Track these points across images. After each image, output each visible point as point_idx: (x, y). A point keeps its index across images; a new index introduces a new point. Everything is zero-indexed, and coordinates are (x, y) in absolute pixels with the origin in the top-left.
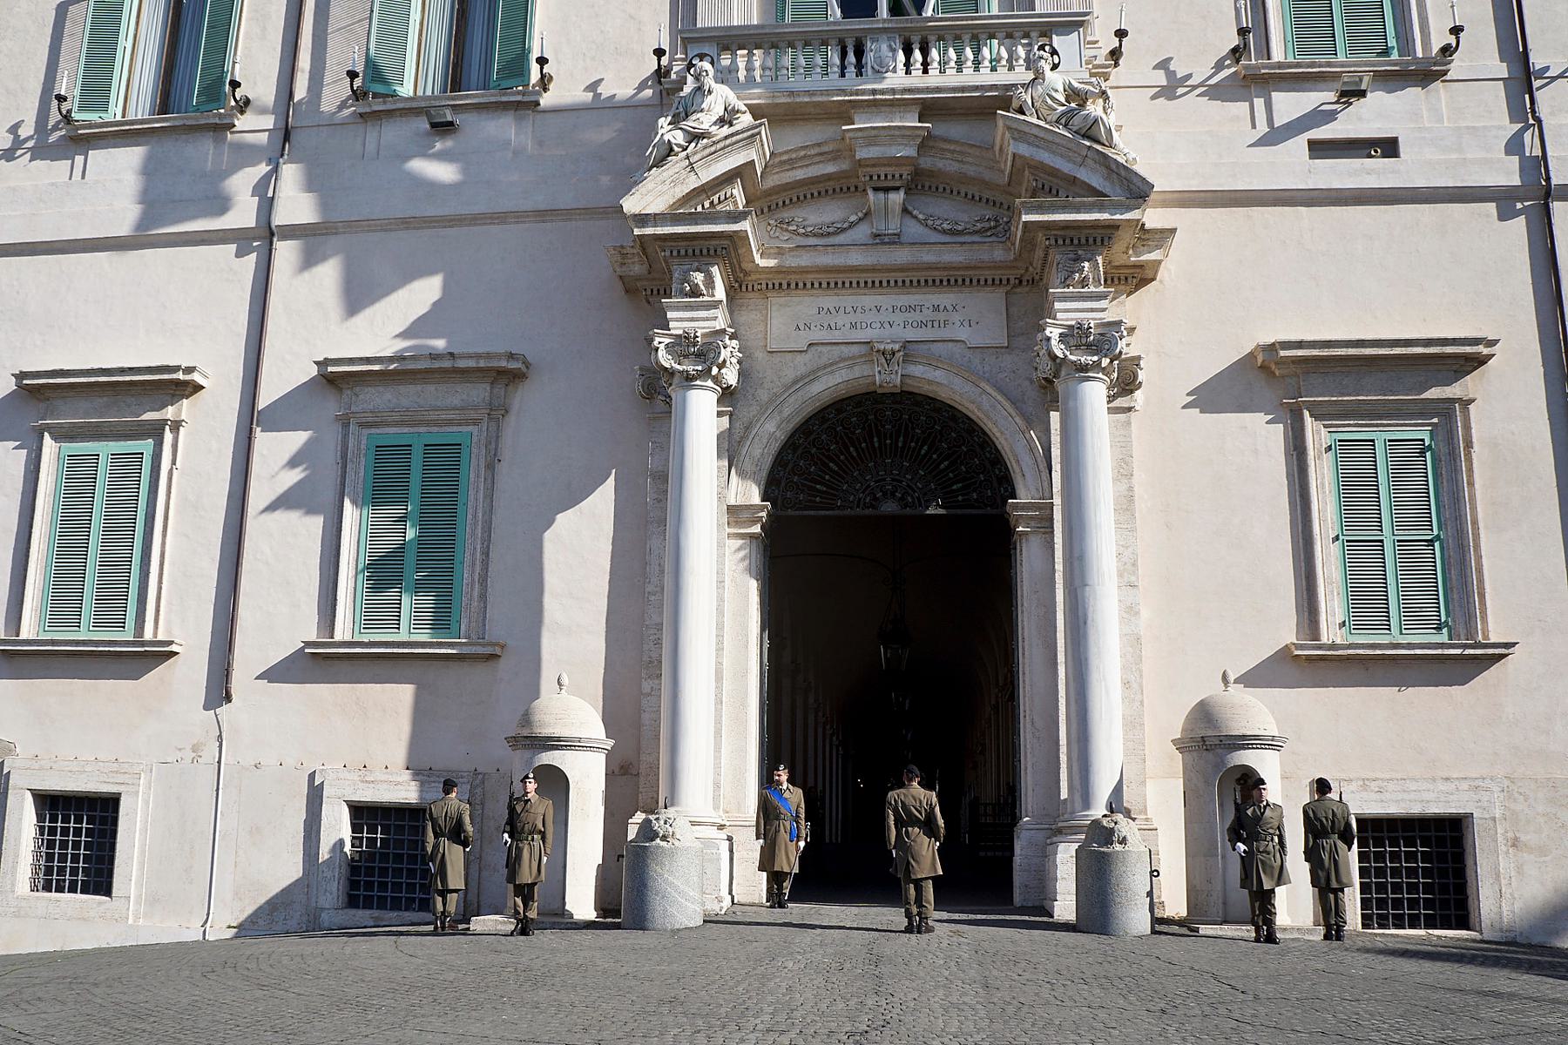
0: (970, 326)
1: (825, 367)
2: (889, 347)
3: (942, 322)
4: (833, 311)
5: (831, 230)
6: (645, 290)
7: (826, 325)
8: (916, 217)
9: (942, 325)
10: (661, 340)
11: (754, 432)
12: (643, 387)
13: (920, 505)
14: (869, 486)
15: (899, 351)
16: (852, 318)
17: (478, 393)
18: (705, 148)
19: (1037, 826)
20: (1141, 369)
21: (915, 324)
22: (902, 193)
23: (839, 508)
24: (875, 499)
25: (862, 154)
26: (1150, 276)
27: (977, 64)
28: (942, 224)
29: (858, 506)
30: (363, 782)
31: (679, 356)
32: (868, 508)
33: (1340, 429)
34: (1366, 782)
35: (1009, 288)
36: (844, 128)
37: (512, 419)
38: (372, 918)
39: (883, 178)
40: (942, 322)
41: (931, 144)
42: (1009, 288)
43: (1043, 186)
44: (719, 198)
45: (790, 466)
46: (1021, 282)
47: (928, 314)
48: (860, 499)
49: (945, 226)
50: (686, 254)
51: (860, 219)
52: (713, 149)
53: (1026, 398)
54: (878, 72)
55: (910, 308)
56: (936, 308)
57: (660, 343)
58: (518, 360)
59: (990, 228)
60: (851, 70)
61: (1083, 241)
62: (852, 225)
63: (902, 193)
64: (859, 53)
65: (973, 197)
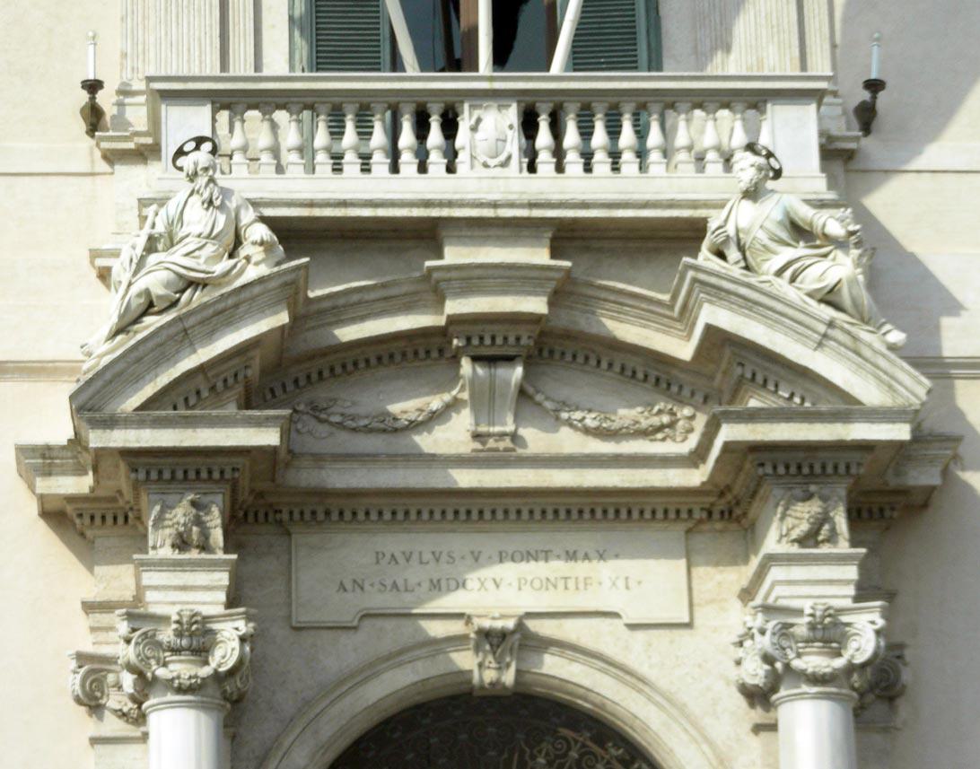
0: (627, 588)
2: (499, 624)
3: (581, 580)
6: (80, 516)
7: (389, 583)
9: (581, 586)
15: (513, 632)
21: (537, 584)
28: (584, 418)
35: (690, 524)
39: (488, 341)
40: (581, 580)
42: (690, 524)
43: (754, 375)
44: (225, 380)
46: (710, 514)
50: (173, 478)
54: (486, 165)
57: (134, 630)
59: (661, 428)
60: (436, 160)
61: (818, 469)
64: (450, 128)
65: (634, 373)
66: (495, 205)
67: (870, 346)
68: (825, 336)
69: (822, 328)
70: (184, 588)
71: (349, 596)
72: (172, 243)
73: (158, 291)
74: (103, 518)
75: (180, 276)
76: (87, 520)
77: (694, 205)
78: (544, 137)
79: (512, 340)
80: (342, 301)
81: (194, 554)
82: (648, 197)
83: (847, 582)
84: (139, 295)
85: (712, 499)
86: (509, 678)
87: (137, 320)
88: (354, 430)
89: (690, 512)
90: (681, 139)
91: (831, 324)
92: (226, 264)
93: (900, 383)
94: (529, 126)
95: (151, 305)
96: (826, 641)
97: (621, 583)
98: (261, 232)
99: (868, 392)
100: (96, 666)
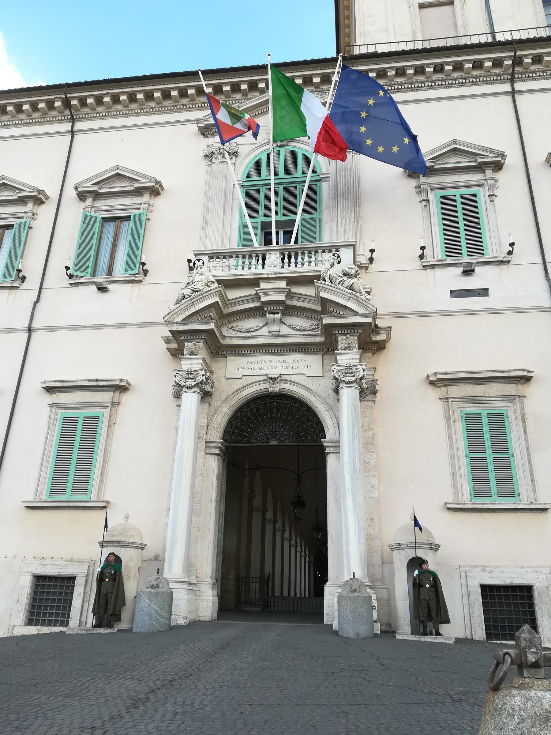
1: (248, 385)
2: (273, 376)
4: (253, 362)
5: (252, 330)
7: (250, 369)
8: (286, 325)
9: (296, 368)
10: (177, 372)
11: (218, 411)
12: (174, 393)
13: (287, 442)
15: (278, 378)
17: (107, 396)
18: (198, 296)
19: (333, 586)
20: (378, 384)
21: (285, 368)
22: (280, 314)
24: (268, 439)
25: (263, 299)
26: (383, 347)
27: (310, 263)
28: (296, 327)
29: (261, 442)
30: (41, 565)
31: (185, 379)
33: (466, 409)
36: (255, 289)
37: (121, 407)
38: (37, 630)
41: (292, 295)
43: (334, 310)
45: (234, 425)
46: (328, 350)
47: (291, 363)
48: (262, 439)
49: (297, 328)
51: (264, 326)
52: (201, 297)
53: (330, 397)
56: (294, 361)
57: (177, 374)
58: (124, 382)
59: (316, 328)
62: (261, 328)
63: (280, 314)
64: (264, 259)
67: (361, 299)
68: (350, 297)
69: (349, 295)
70: (191, 364)
79: (278, 308)
80: (237, 300)
81: (194, 356)
83: (357, 359)
84: (181, 294)
86: (277, 390)
87: (181, 301)
89: (323, 349)
90: (320, 258)
91: (351, 294)
92: (203, 288)
93: (369, 308)
96: (351, 373)
97: (306, 367)
99: (361, 310)
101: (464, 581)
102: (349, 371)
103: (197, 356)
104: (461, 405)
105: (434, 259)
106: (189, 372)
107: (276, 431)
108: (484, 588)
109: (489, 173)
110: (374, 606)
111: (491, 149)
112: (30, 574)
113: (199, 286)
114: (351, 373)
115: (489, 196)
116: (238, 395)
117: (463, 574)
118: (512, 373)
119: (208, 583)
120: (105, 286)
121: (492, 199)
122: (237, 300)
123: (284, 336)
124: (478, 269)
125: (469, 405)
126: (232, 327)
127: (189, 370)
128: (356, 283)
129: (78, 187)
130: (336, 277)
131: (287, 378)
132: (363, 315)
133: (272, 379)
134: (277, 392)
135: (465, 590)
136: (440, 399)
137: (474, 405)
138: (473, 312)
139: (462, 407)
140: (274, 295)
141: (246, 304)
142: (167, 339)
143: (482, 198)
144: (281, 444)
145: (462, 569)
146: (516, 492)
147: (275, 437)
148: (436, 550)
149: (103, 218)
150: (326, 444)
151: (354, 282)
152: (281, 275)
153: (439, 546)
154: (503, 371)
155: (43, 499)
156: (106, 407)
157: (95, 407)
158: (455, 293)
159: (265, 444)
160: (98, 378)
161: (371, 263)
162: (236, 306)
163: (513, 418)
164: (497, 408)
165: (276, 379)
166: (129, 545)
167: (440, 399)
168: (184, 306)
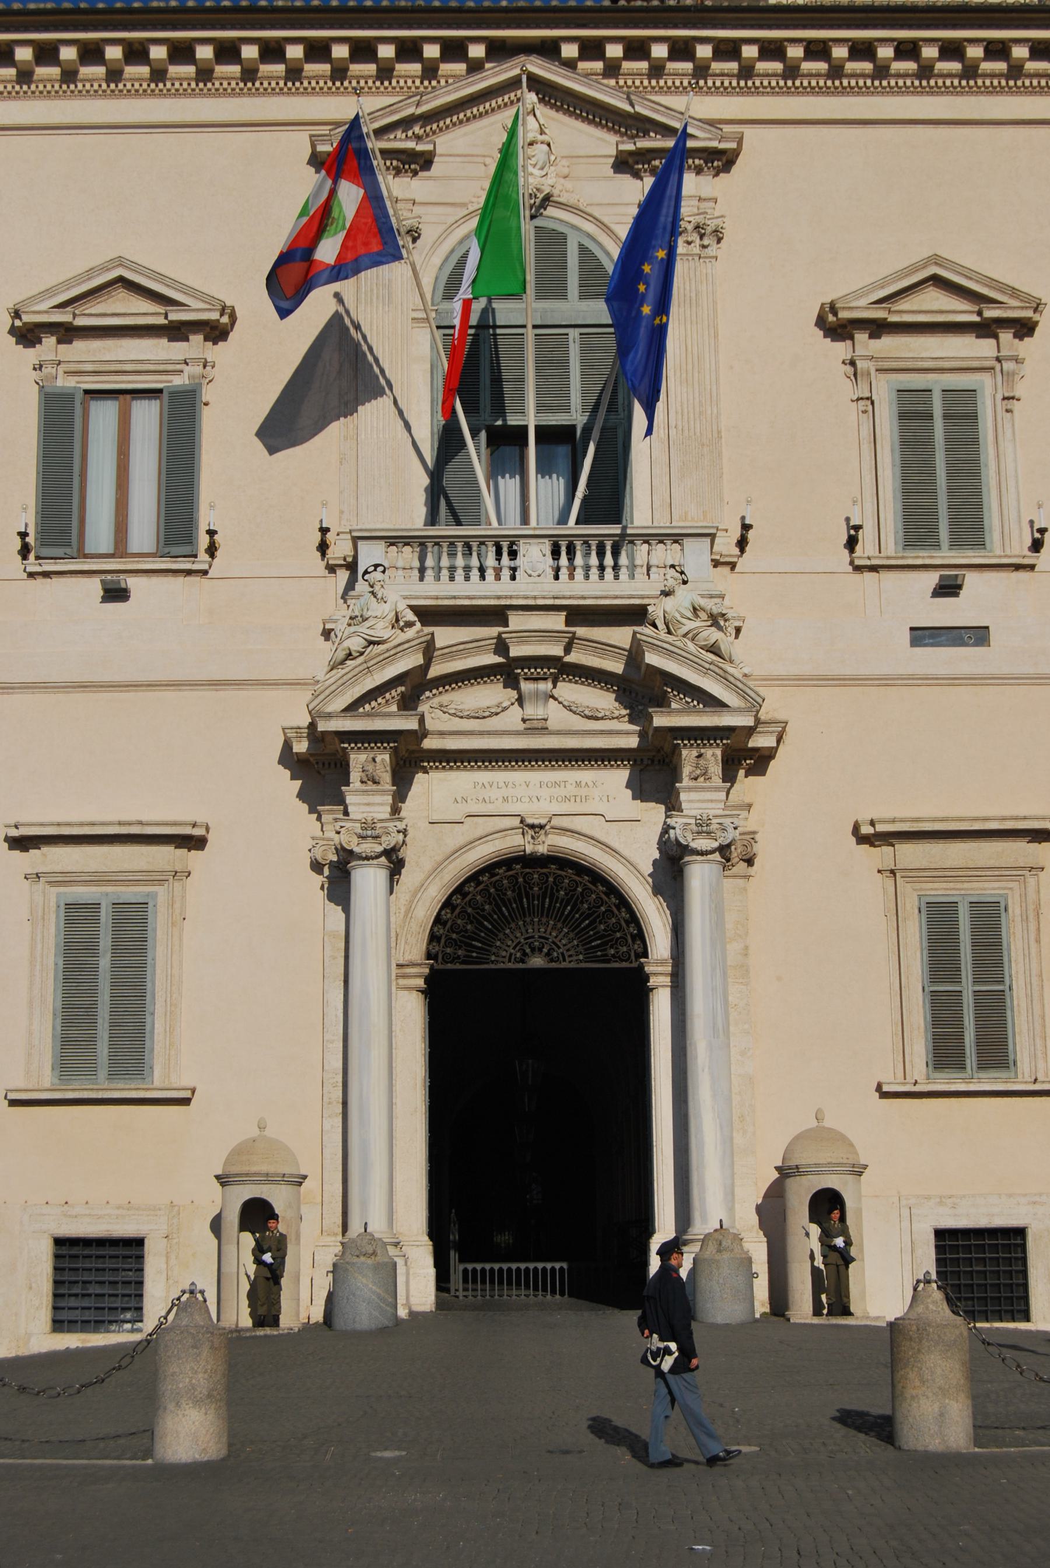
2: (536, 822)
3: (583, 797)
5: (487, 714)
6: (317, 763)
7: (481, 799)
9: (584, 800)
10: (343, 824)
13: (564, 960)
14: (519, 943)
16: (505, 792)
21: (560, 799)
23: (492, 962)
24: (525, 954)
25: (515, 651)
29: (510, 961)
30: (65, 1215)
32: (518, 962)
34: (944, 1200)
40: (583, 797)
46: (653, 761)
47: (571, 790)
49: (587, 712)
54: (530, 576)
55: (556, 784)
56: (578, 784)
57: (342, 827)
64: (513, 554)
66: (535, 598)
70: (368, 804)
71: (459, 805)
72: (365, 620)
73: (353, 648)
74: (329, 764)
75: (365, 639)
76: (321, 765)
77: (642, 597)
78: (564, 560)
80: (454, 649)
82: (617, 593)
84: (343, 650)
85: (654, 754)
86: (542, 849)
87: (342, 662)
88: (462, 717)
89: (642, 760)
94: (556, 553)
95: (350, 654)
97: (605, 799)
98: (411, 616)
100: (325, 842)
101: (906, 1224)
102: (705, 829)
103: (379, 787)
104: (918, 886)
105: (880, 552)
106: (366, 825)
107: (540, 937)
108: (941, 1234)
109: (1006, 336)
110: (755, 1273)
111: (1014, 289)
112: (46, 1235)
113: (382, 630)
114: (709, 833)
115: (1004, 399)
116: (458, 860)
117: (905, 1212)
118: (1022, 823)
119: (423, 1243)
120: (123, 586)
121: (1009, 407)
122: (454, 649)
123: (559, 733)
124: (972, 581)
125: (936, 885)
126: (441, 706)
127: (369, 821)
128: (723, 641)
129: (23, 312)
130: (679, 618)
131: (565, 822)
132: (738, 710)
133: (532, 827)
134: (543, 854)
135: (907, 1239)
136: (879, 871)
137: (944, 885)
138: (954, 680)
139: (921, 889)
140: (542, 644)
141: (474, 656)
142: (297, 733)
143: (989, 403)
144: (554, 965)
145: (904, 1202)
146: (1011, 1057)
147: (540, 950)
148: (860, 1174)
149: (87, 392)
150: (651, 968)
151: (720, 640)
152: (558, 602)
153: (865, 1167)
154: (1004, 819)
155: (47, 1085)
156: (161, 882)
157: (137, 882)
158: (921, 636)
159: (521, 966)
160: (144, 818)
161: (742, 550)
162: (452, 660)
163: (1018, 911)
164: (988, 889)
165: (542, 827)
166: (286, 1179)
167: (879, 871)
168: (350, 676)
